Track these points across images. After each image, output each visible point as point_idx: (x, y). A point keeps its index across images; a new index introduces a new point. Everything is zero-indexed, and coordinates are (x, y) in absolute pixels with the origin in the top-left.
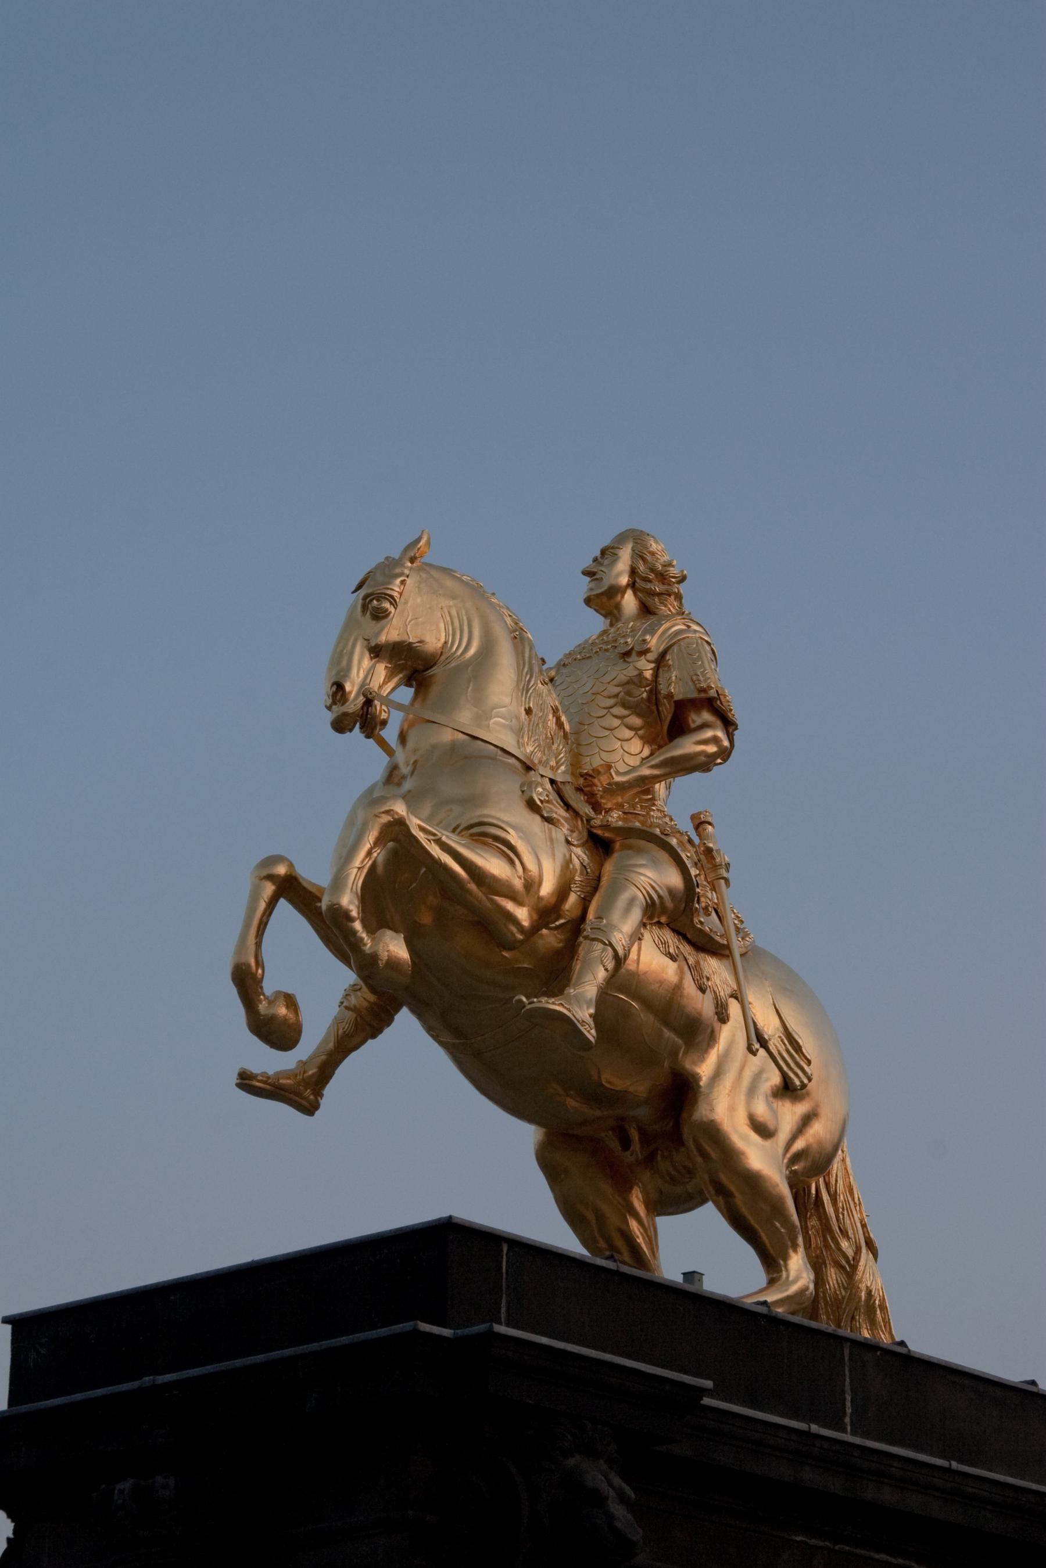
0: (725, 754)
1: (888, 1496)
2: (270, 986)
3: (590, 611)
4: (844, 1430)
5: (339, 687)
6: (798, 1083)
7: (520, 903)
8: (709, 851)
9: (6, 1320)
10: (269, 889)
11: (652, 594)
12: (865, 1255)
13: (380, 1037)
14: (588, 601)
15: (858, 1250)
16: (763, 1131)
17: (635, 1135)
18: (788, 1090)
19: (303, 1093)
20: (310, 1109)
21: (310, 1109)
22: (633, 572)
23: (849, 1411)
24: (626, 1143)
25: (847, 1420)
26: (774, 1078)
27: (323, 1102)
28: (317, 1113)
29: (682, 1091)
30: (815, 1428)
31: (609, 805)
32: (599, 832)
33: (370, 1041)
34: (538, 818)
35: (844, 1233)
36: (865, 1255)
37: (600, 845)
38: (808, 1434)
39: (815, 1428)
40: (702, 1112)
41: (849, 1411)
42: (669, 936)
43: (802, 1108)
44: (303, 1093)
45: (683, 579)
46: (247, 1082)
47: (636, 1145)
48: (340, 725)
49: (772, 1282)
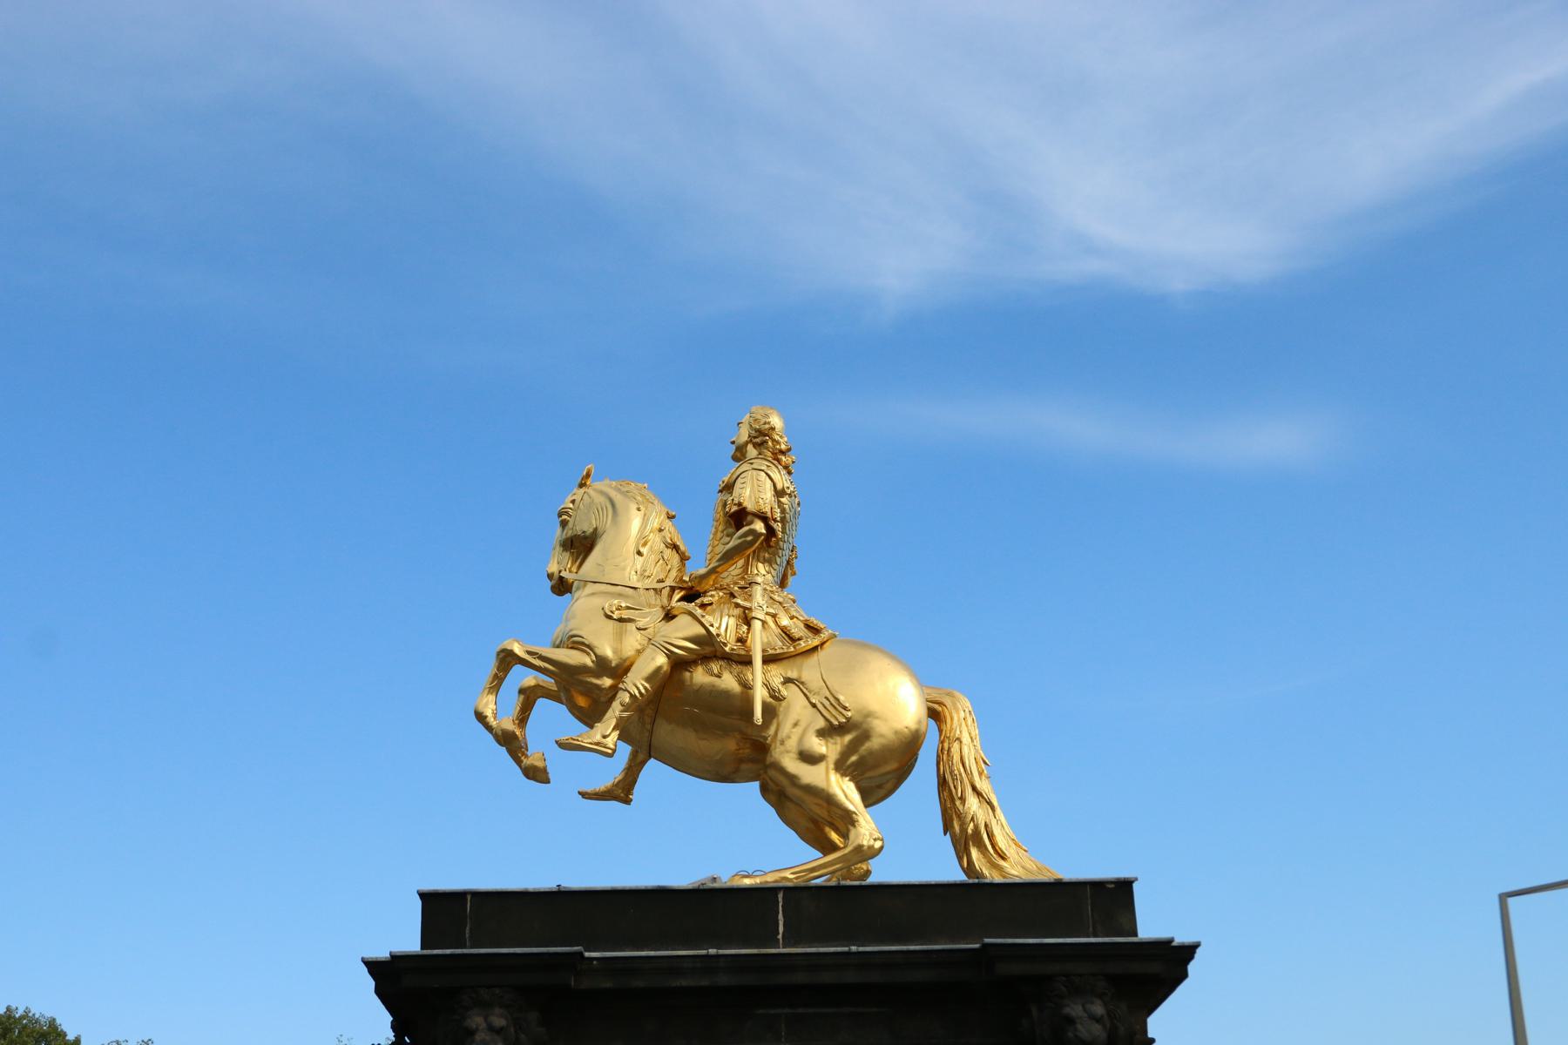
1: (800, 978)
7: (598, 676)
12: (973, 804)
18: (829, 731)
19: (622, 792)
20: (627, 801)
23: (781, 929)
26: (821, 723)
38: (708, 956)
39: (712, 951)
43: (848, 738)
46: (584, 795)
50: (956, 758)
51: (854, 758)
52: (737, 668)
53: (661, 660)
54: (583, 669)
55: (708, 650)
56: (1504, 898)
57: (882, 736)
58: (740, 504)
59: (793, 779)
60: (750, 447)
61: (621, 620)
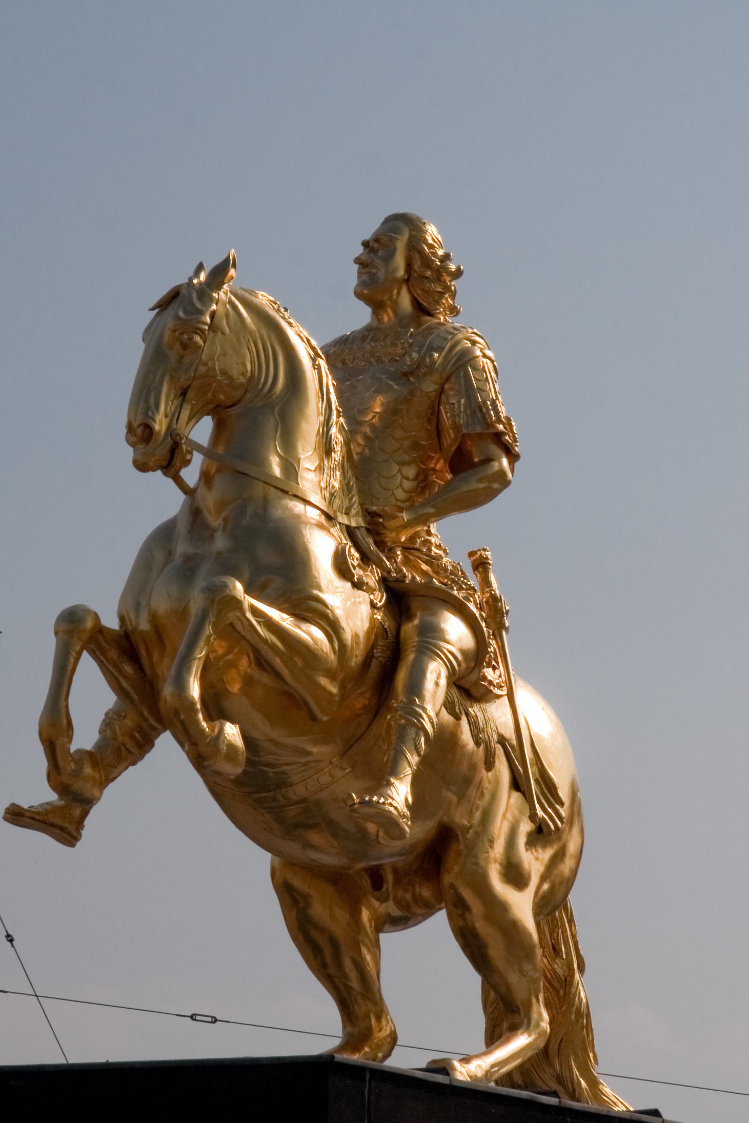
3: (361, 304)
5: (148, 428)
6: (552, 827)
11: (427, 292)
13: (140, 763)
17: (390, 877)
18: (541, 834)
19: (63, 820)
22: (409, 266)
27: (84, 832)
28: (78, 844)
32: (393, 585)
33: (131, 768)
34: (349, 585)
45: (458, 274)
46: (16, 815)
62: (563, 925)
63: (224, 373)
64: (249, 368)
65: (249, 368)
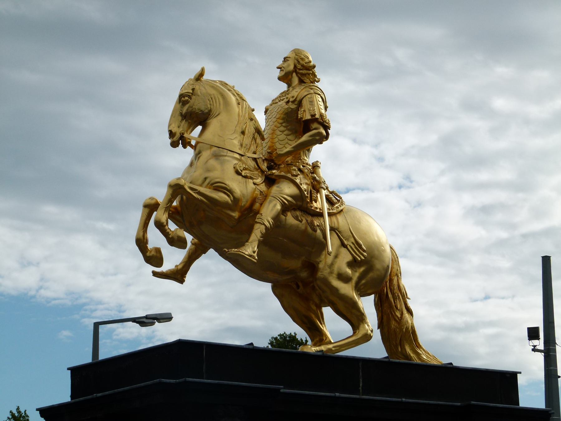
0: (327, 137)
2: (150, 246)
4: (357, 392)
6: (359, 259)
7: (233, 211)
8: (314, 179)
9: (68, 369)
10: (147, 210)
12: (406, 315)
14: (280, 79)
15: (402, 314)
16: (345, 279)
19: (178, 275)
20: (181, 281)
21: (181, 281)
22: (295, 66)
23: (361, 385)
24: (298, 287)
25: (360, 388)
26: (349, 258)
29: (313, 268)
30: (337, 394)
31: (280, 163)
32: (270, 176)
35: (397, 308)
36: (406, 315)
37: (270, 181)
39: (337, 394)
40: (319, 274)
41: (361, 385)
42: (298, 213)
43: (362, 269)
44: (178, 275)
46: (155, 274)
47: (301, 287)
48: (174, 145)
49: (354, 333)
50: (396, 287)
51: (363, 282)
52: (310, 218)
53: (279, 207)
54: (225, 205)
55: (299, 203)
56: (97, 326)
57: (378, 270)
58: (313, 116)
59: (335, 291)
60: (294, 74)
61: (246, 177)
62: (399, 298)
63: (199, 109)
64: (209, 106)
65: (209, 106)
